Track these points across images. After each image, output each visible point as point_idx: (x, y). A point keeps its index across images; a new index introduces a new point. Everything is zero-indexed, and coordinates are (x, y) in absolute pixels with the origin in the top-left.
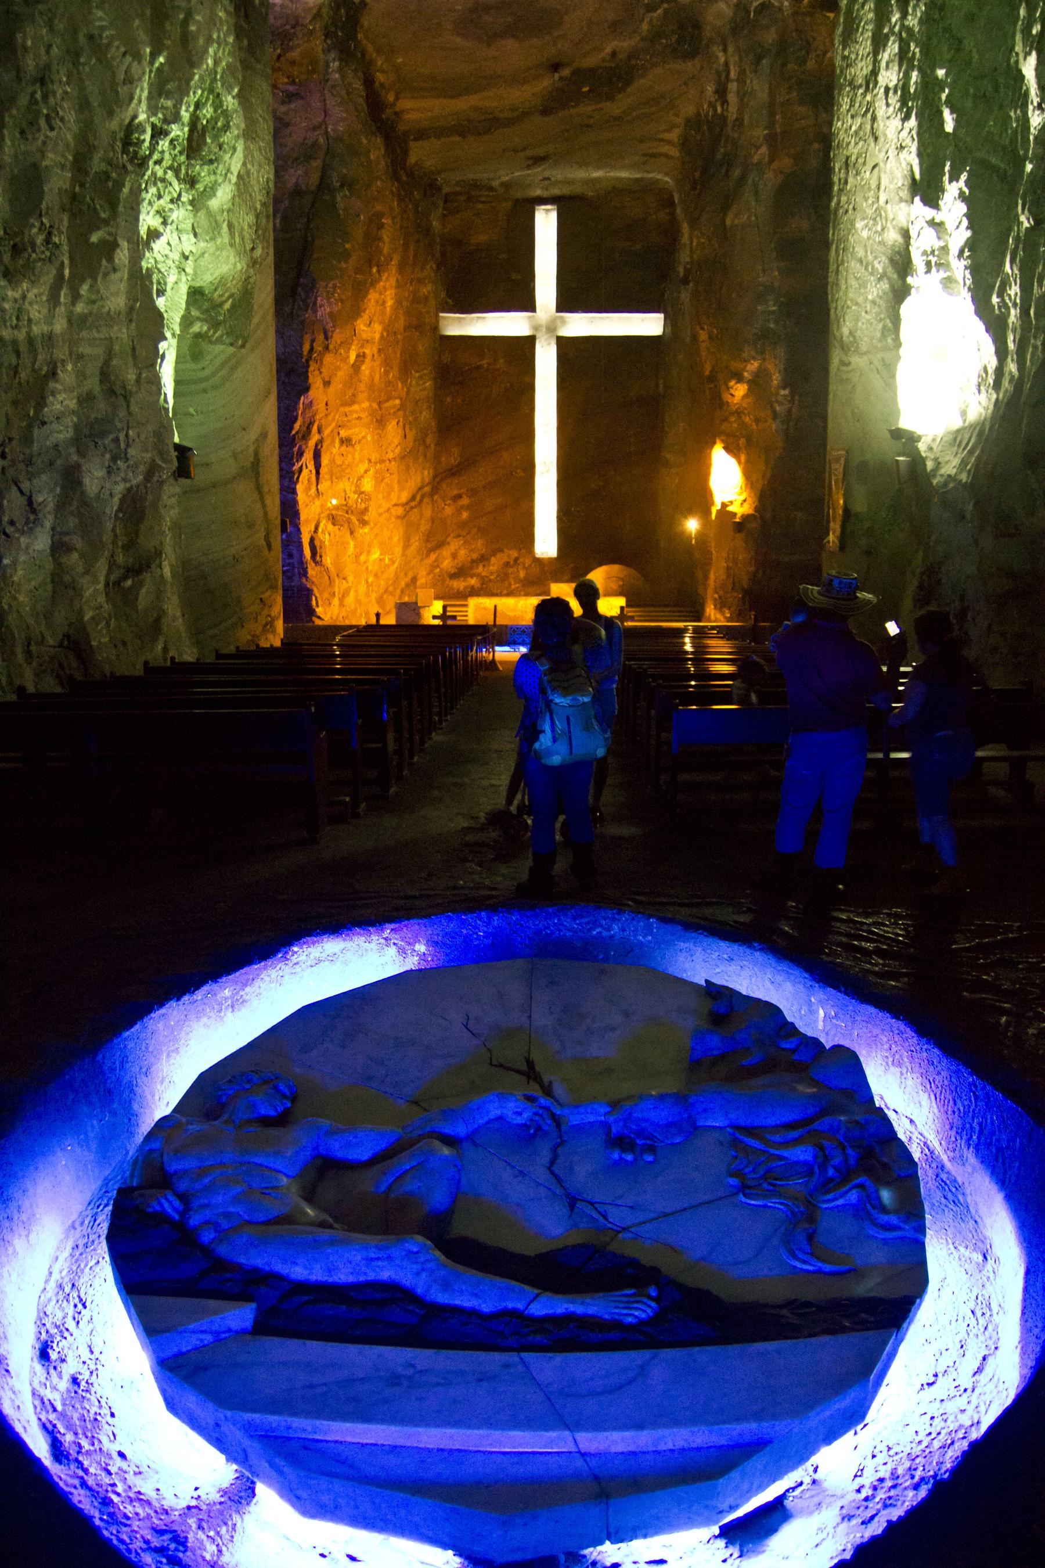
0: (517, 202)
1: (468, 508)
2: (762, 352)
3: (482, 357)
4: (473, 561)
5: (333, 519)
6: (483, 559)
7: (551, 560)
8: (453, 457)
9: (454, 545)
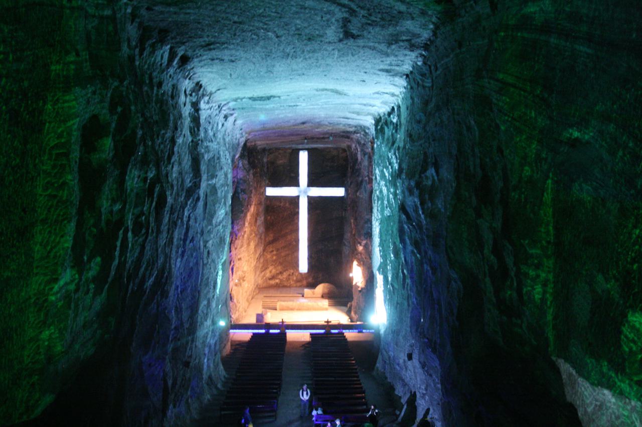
0: (293, 150)
1: (276, 255)
2: (367, 239)
3: (281, 203)
4: (277, 274)
5: (236, 285)
6: (281, 273)
7: (305, 274)
8: (271, 237)
9: (271, 268)
